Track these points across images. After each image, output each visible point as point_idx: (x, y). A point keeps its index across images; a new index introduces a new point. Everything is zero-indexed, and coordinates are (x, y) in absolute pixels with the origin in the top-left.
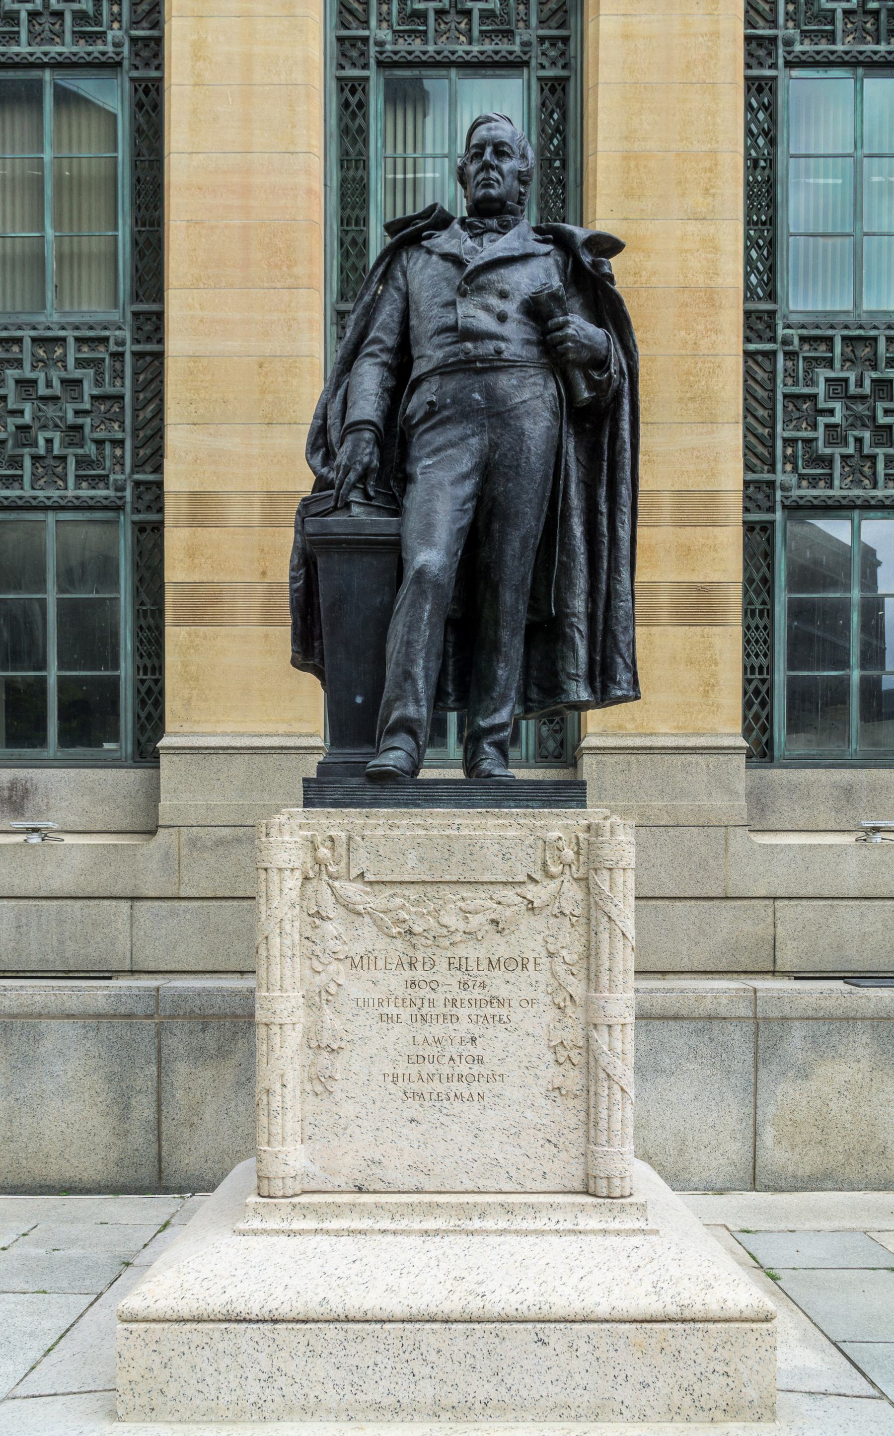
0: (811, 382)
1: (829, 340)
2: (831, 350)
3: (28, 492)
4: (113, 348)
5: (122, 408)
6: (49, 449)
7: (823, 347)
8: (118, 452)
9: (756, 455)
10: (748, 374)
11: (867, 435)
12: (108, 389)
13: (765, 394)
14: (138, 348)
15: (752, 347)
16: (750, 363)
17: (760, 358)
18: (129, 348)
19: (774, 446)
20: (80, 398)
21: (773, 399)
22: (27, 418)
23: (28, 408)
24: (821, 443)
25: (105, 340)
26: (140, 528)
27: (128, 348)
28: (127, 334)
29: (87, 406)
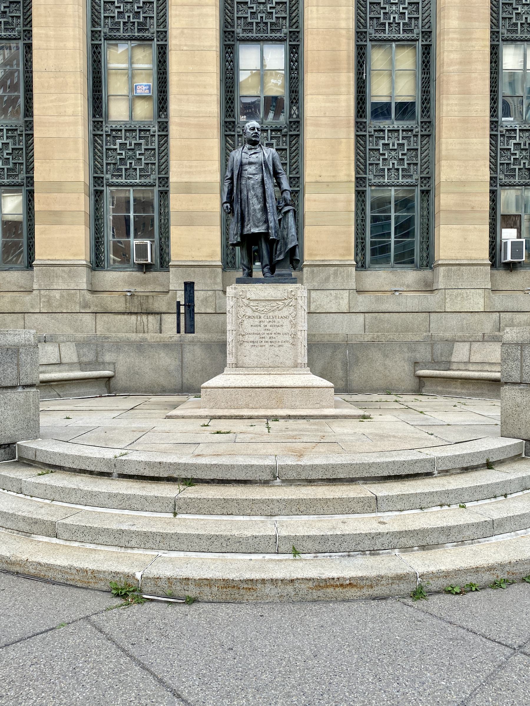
0: (377, 145)
1: (383, 131)
2: (384, 134)
3: (124, 181)
4: (152, 133)
5: (155, 153)
6: (131, 166)
7: (382, 133)
8: (153, 167)
9: (360, 168)
10: (357, 142)
11: (396, 162)
12: (149, 147)
13: (363, 149)
14: (160, 133)
15: (359, 133)
16: (359, 138)
17: (361, 137)
18: (157, 134)
19: (366, 166)
20: (140, 150)
21: (365, 150)
22: (123, 157)
23: (124, 153)
24: (381, 165)
25: (149, 130)
26: (161, 192)
27: (157, 134)
28: (156, 128)
29: (143, 152)
